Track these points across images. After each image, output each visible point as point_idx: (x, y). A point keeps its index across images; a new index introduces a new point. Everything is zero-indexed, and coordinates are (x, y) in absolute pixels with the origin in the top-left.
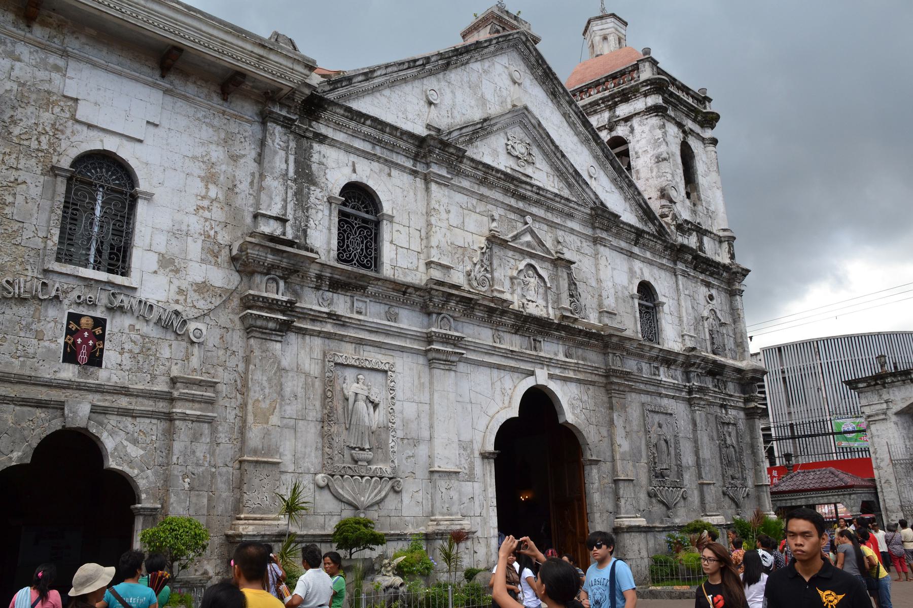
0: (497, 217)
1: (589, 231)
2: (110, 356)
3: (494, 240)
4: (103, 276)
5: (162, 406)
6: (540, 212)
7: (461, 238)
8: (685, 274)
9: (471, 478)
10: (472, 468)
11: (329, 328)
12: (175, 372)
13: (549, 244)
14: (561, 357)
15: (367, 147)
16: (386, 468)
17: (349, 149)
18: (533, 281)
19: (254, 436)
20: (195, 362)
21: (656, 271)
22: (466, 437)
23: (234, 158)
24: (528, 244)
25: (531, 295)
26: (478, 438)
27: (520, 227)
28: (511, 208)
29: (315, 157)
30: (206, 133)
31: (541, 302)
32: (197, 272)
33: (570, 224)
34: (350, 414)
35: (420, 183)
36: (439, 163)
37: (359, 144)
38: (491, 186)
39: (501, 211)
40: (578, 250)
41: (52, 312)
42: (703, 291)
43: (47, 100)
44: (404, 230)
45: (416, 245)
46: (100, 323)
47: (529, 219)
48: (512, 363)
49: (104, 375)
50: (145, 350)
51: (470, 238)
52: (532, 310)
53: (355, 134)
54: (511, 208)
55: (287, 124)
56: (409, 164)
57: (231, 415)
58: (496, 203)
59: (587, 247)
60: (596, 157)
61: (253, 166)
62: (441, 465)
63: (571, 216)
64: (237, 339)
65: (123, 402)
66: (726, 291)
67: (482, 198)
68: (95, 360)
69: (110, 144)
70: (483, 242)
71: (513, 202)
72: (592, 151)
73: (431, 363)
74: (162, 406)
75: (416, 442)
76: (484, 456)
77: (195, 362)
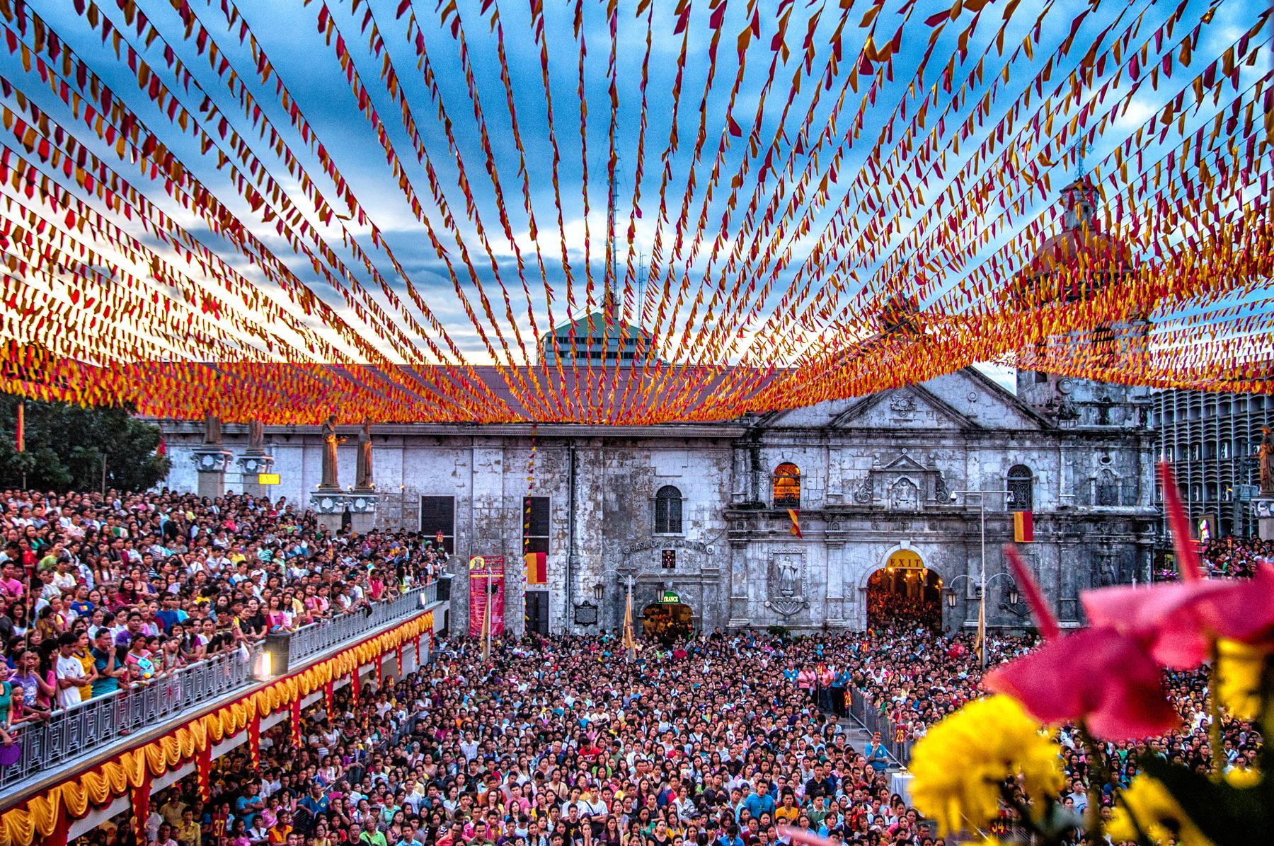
0: (877, 455)
1: (963, 442)
2: (678, 564)
3: (872, 472)
4: (672, 535)
5: (698, 580)
6: (918, 442)
7: (850, 475)
8: (1067, 449)
9: (852, 600)
10: (853, 595)
11: (771, 538)
12: (703, 566)
13: (922, 461)
14: (927, 530)
15: (791, 441)
16: (800, 598)
17: (779, 446)
18: (906, 488)
19: (735, 589)
20: (710, 562)
21: (1035, 455)
22: (849, 580)
23: (721, 470)
24: (903, 466)
25: (904, 496)
26: (857, 581)
27: (898, 456)
28: (891, 447)
29: (761, 456)
30: (707, 462)
31: (912, 498)
32: (708, 525)
33: (943, 442)
34: (781, 574)
35: (824, 451)
36: (835, 437)
37: (785, 441)
38: (875, 438)
39: (883, 450)
40: (950, 458)
41: (656, 551)
42: (1096, 456)
43: (646, 471)
44: (814, 480)
45: (821, 486)
46: (673, 552)
47: (904, 450)
48: (885, 539)
49: (678, 570)
50: (690, 560)
51: (857, 473)
52: (903, 506)
53: (783, 437)
54: (891, 447)
55: (745, 447)
56: (816, 442)
57: (726, 580)
58: (879, 446)
59: (958, 455)
60: (978, 385)
61: (730, 471)
62: (831, 596)
63: (944, 438)
64: (727, 550)
65: (683, 580)
66: (1133, 449)
67: (867, 447)
68: (673, 566)
69: (669, 483)
70: (866, 473)
71: (893, 442)
72: (974, 382)
73: (828, 546)
74: (698, 580)
75: (818, 585)
76: (861, 590)
77: (710, 562)
